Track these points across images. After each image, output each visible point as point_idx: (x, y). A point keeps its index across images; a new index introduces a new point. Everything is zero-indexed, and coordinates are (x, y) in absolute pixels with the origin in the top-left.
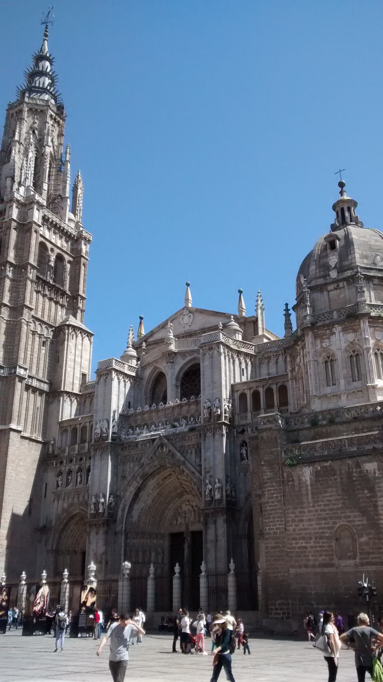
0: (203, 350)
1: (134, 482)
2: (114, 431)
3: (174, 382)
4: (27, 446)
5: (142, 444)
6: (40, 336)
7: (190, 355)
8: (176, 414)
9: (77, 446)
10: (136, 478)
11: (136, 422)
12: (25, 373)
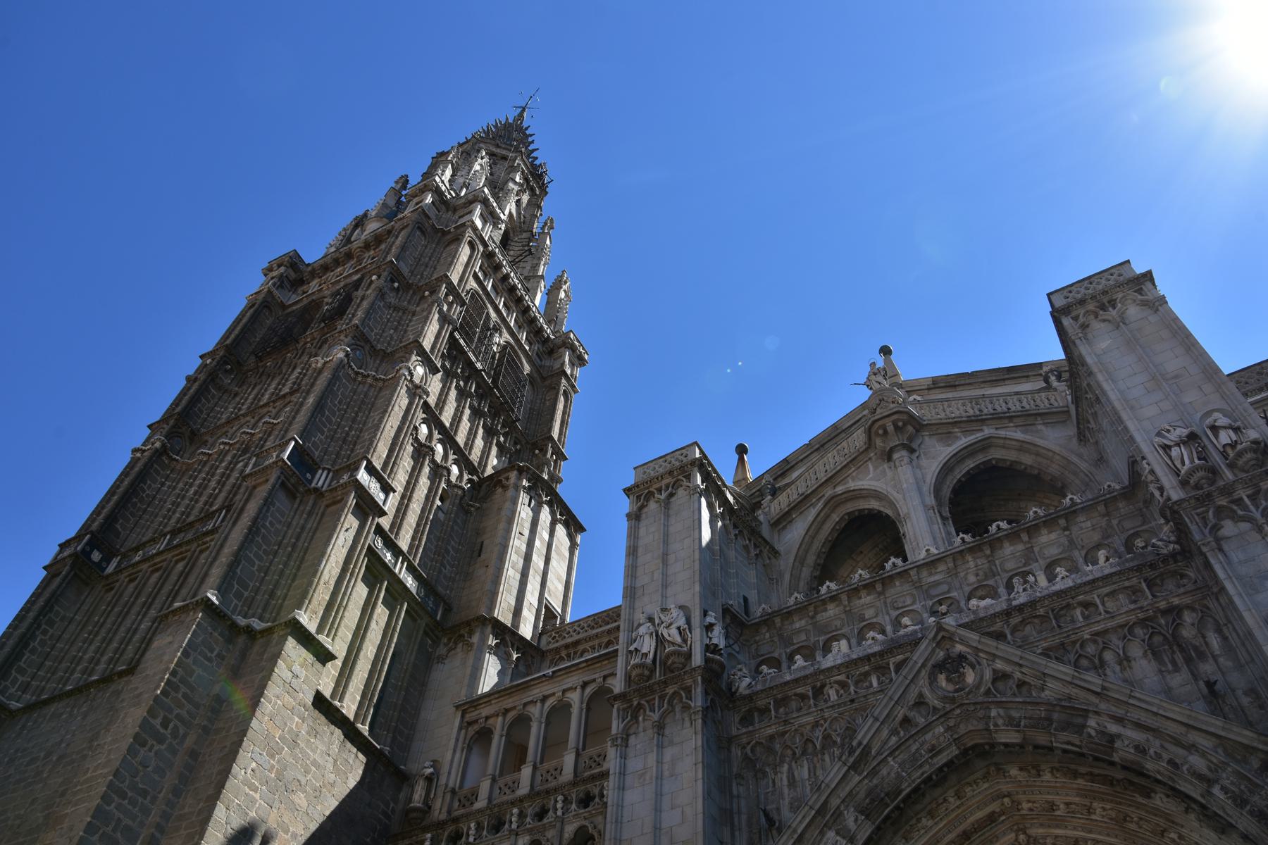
0: (1076, 319)
1: (831, 834)
2: (715, 641)
3: (931, 500)
4: (335, 748)
5: (843, 685)
6: (438, 471)
7: (966, 433)
8: (972, 579)
9: (526, 772)
10: (838, 814)
11: (787, 641)
12: (382, 496)
